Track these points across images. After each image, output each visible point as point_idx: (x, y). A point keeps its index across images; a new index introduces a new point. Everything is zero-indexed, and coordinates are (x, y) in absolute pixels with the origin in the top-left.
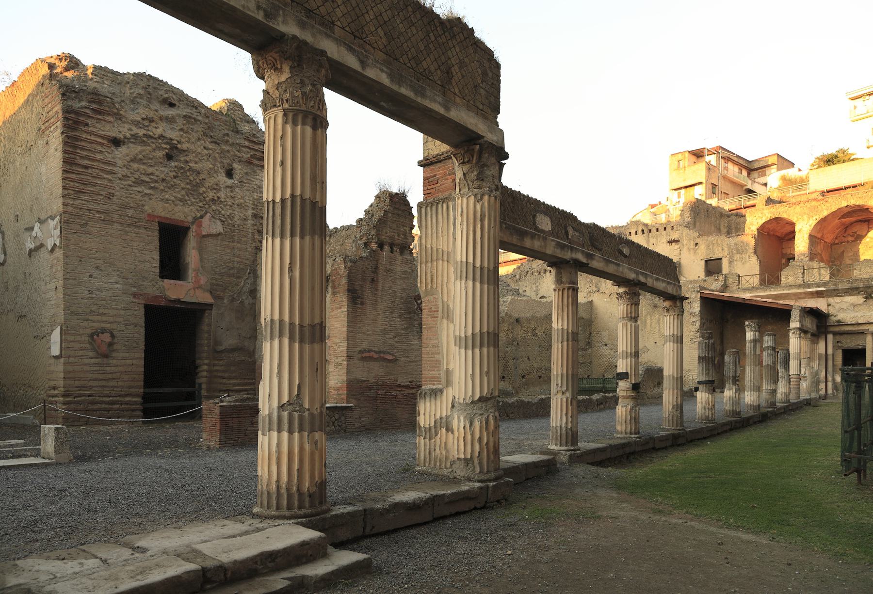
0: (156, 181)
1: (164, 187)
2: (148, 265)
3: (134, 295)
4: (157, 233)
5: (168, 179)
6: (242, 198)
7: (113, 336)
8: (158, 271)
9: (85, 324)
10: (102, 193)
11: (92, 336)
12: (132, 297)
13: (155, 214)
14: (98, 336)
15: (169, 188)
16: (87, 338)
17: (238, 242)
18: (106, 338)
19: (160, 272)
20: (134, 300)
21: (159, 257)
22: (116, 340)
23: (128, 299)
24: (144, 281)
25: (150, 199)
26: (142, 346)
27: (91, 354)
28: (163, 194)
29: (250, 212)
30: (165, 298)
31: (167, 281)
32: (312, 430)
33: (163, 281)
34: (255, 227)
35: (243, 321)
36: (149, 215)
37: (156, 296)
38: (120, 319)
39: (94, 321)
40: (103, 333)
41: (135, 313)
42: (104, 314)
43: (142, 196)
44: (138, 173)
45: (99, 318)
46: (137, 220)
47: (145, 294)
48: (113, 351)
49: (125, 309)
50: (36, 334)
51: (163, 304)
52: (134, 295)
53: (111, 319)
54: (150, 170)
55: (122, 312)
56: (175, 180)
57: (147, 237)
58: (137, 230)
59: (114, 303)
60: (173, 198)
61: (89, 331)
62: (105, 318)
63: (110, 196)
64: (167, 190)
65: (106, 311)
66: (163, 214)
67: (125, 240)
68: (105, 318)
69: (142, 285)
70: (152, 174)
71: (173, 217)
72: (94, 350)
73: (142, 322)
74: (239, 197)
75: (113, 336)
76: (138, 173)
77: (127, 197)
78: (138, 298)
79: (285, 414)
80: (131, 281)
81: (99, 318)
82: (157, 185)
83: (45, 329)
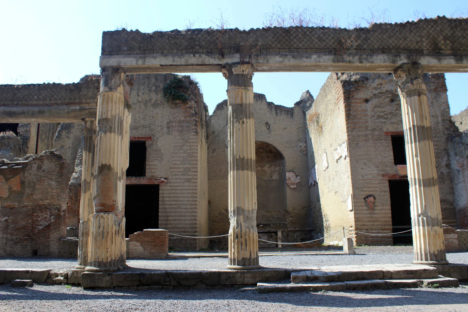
0: (387, 114)
1: (392, 116)
2: (388, 159)
3: (383, 175)
4: (390, 141)
5: (393, 112)
6: (434, 112)
7: (375, 198)
8: (393, 161)
9: (362, 193)
10: (363, 126)
11: (365, 199)
12: (382, 176)
13: (388, 131)
14: (368, 199)
15: (394, 116)
16: (363, 200)
17: (435, 137)
18: (371, 199)
19: (395, 161)
20: (383, 178)
21: (393, 154)
22: (376, 200)
23: (381, 178)
24: (387, 167)
25: (385, 124)
26: (389, 202)
27: (366, 208)
28: (392, 120)
29: (440, 119)
30: (398, 175)
31: (398, 166)
32: (433, 225)
33: (396, 166)
34: (444, 127)
35: (444, 183)
36: (386, 133)
37: (394, 175)
38: (378, 189)
39: (365, 191)
40: (370, 197)
41: (384, 185)
42: (370, 187)
43: (381, 123)
44: (378, 113)
45: (367, 189)
46: (380, 136)
47: (388, 174)
48: (375, 206)
49: (379, 183)
50: (342, 200)
51: (397, 179)
52: (383, 175)
53: (373, 189)
54: (383, 109)
55: (378, 185)
56: (396, 111)
57: (386, 144)
58: (381, 142)
59: (374, 181)
60: (396, 121)
61: (364, 197)
62: (370, 189)
63: (367, 127)
64: (393, 117)
65: (371, 186)
66: (392, 130)
67: (376, 148)
68: (370, 189)
69: (386, 170)
70: (385, 111)
71: (397, 131)
72: (367, 206)
73: (387, 189)
74: (433, 111)
75: (375, 198)
76: (378, 113)
77: (374, 126)
78: (385, 177)
79: (420, 218)
80: (380, 168)
81: (367, 189)
82: (388, 116)
83: (345, 197)
